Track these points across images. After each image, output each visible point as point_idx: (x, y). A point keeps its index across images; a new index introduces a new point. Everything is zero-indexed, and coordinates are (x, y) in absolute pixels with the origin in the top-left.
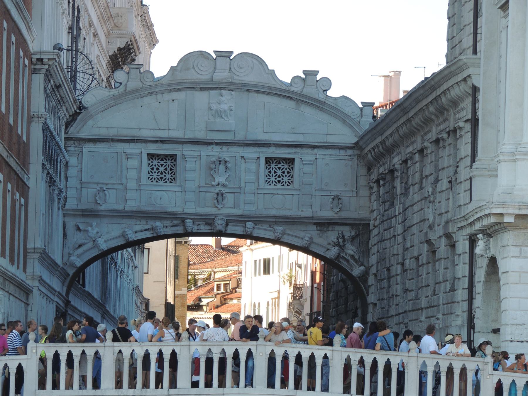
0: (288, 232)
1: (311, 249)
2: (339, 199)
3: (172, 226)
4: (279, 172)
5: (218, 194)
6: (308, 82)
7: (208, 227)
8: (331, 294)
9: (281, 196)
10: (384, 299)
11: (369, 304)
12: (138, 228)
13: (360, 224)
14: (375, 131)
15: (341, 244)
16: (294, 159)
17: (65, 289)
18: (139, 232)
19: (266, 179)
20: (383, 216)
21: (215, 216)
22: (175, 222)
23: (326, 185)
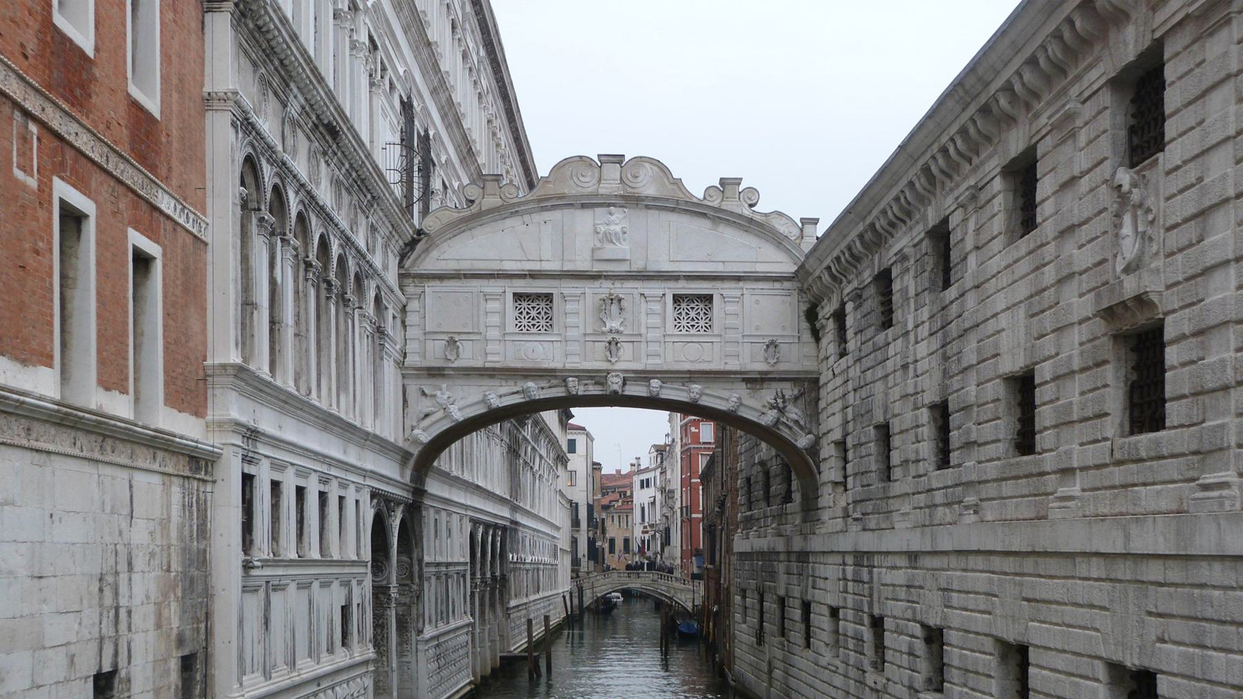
0: (708, 391)
1: (739, 413)
2: (776, 346)
3: (550, 387)
4: (693, 314)
5: (610, 343)
6: (728, 193)
7: (599, 388)
8: (739, 482)
9: (697, 345)
10: (871, 472)
11: (824, 483)
12: (503, 390)
13: (804, 380)
14: (852, 215)
15: (781, 405)
16: (711, 296)
17: (408, 473)
18: (505, 395)
19: (676, 323)
20: (860, 351)
21: (608, 372)
22: (554, 382)
23: (757, 328)
